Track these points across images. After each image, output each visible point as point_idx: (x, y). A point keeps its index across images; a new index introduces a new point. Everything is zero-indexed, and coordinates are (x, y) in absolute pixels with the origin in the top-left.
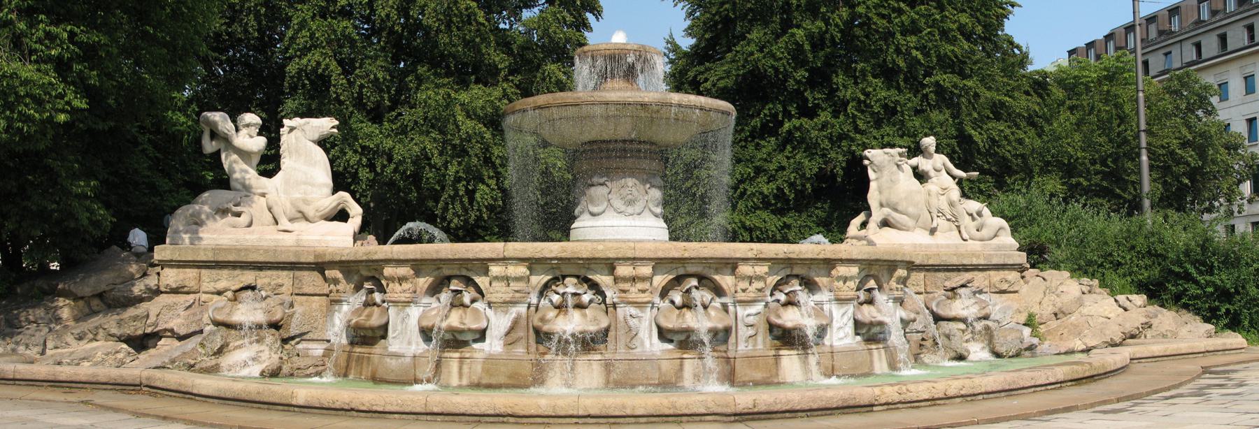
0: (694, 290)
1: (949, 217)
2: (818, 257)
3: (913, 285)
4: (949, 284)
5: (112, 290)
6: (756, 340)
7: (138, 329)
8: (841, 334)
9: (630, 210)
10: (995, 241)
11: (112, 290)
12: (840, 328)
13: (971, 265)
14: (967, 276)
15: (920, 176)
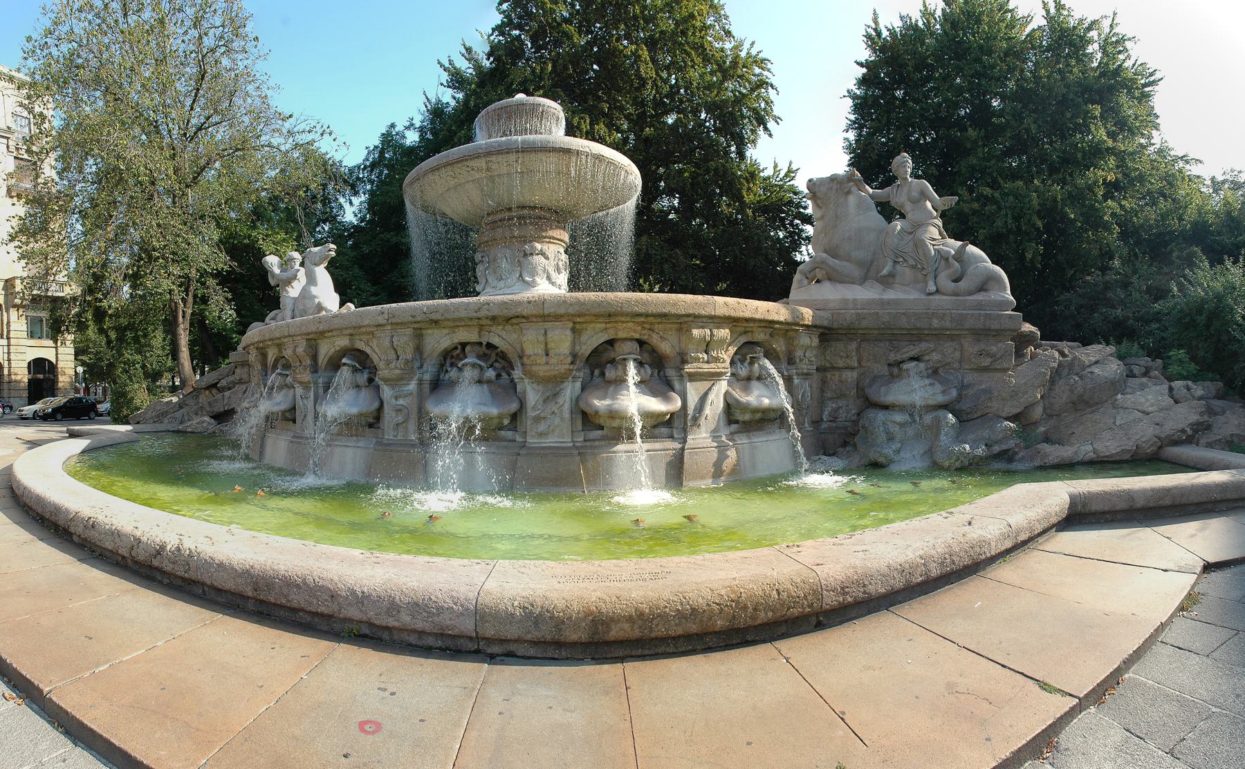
0: (468, 368)
1: (911, 262)
2: (475, 315)
3: (842, 357)
4: (893, 357)
5: (217, 383)
6: (406, 429)
7: (219, 408)
8: (542, 427)
9: (502, 284)
10: (980, 297)
11: (217, 383)
12: (537, 419)
13: (930, 329)
14: (924, 346)
15: (888, 211)
